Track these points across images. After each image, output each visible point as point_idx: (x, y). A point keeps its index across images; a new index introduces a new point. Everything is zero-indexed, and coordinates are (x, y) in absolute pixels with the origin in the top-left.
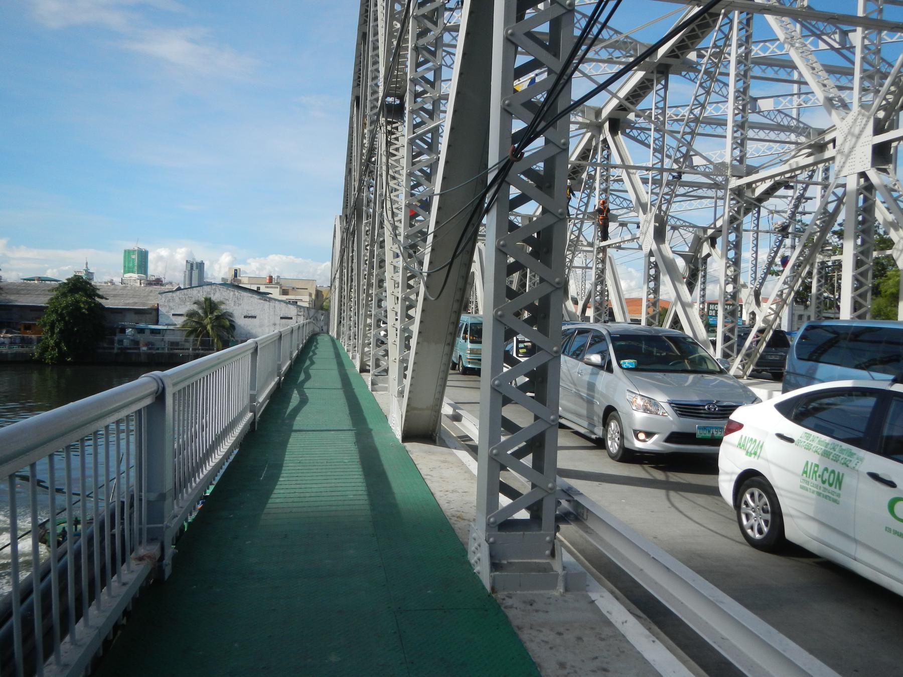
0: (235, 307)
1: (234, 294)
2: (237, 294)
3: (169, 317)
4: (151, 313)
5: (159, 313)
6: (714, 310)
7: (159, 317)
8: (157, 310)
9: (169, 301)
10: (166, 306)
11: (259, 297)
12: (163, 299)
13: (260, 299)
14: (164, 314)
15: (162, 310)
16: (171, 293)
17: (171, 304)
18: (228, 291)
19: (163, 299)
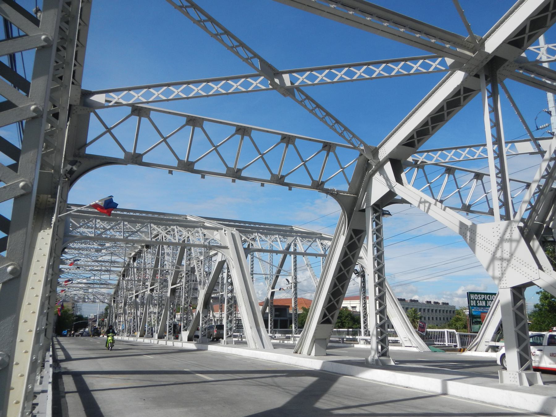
6: (475, 300)
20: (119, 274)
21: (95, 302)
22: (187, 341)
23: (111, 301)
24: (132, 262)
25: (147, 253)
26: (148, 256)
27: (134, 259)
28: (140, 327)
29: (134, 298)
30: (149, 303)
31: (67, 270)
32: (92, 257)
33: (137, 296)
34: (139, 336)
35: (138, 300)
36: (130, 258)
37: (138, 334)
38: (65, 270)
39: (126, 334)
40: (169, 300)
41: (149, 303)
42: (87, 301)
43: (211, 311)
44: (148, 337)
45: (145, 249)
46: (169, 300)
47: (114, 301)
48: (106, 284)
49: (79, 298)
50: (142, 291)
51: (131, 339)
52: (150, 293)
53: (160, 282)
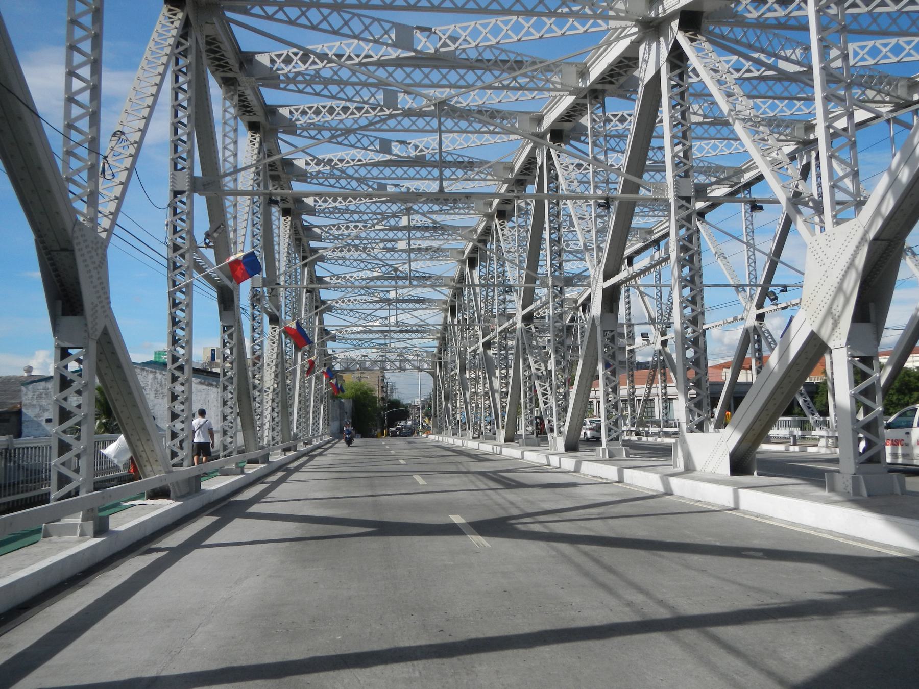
0: (156, 401)
1: (155, 378)
2: (159, 376)
3: (39, 425)
4: (7, 421)
5: (23, 419)
7: (24, 425)
8: (19, 413)
9: (40, 397)
10: (34, 406)
11: (198, 380)
12: (30, 395)
13: (200, 383)
14: (31, 421)
15: (28, 413)
16: (43, 383)
17: (44, 402)
18: (145, 373)
19: (30, 395)
20: (444, 306)
21: (405, 370)
22: (727, 470)
23: (434, 367)
24: (467, 270)
25: (502, 230)
26: (505, 232)
27: (473, 263)
28: (503, 416)
29: (481, 349)
30: (525, 349)
31: (337, 302)
32: (380, 268)
33: (487, 345)
34: (503, 441)
35: (490, 353)
36: (463, 262)
37: (502, 434)
38: (334, 304)
39: (470, 433)
40: (599, 329)
41: (525, 349)
42: (388, 368)
43: (672, 374)
44: (529, 443)
45: (497, 220)
46: (599, 329)
47: (440, 364)
48: (421, 330)
49: (375, 362)
50: (500, 329)
51: (486, 447)
52: (523, 325)
53: (553, 286)
